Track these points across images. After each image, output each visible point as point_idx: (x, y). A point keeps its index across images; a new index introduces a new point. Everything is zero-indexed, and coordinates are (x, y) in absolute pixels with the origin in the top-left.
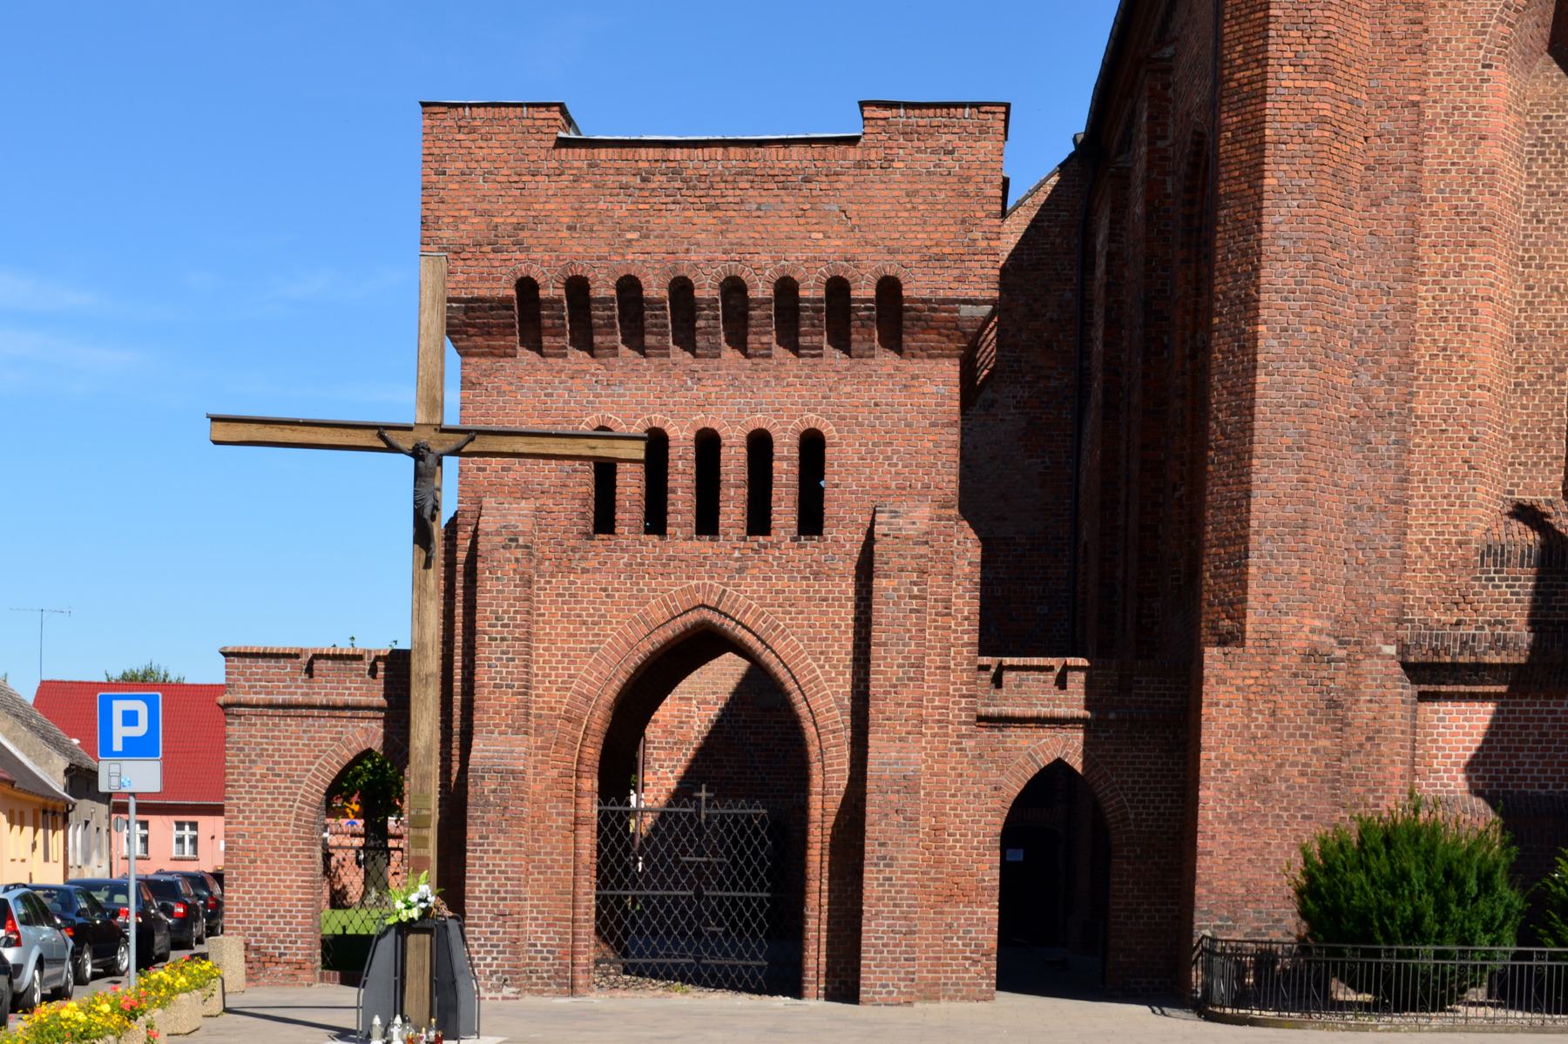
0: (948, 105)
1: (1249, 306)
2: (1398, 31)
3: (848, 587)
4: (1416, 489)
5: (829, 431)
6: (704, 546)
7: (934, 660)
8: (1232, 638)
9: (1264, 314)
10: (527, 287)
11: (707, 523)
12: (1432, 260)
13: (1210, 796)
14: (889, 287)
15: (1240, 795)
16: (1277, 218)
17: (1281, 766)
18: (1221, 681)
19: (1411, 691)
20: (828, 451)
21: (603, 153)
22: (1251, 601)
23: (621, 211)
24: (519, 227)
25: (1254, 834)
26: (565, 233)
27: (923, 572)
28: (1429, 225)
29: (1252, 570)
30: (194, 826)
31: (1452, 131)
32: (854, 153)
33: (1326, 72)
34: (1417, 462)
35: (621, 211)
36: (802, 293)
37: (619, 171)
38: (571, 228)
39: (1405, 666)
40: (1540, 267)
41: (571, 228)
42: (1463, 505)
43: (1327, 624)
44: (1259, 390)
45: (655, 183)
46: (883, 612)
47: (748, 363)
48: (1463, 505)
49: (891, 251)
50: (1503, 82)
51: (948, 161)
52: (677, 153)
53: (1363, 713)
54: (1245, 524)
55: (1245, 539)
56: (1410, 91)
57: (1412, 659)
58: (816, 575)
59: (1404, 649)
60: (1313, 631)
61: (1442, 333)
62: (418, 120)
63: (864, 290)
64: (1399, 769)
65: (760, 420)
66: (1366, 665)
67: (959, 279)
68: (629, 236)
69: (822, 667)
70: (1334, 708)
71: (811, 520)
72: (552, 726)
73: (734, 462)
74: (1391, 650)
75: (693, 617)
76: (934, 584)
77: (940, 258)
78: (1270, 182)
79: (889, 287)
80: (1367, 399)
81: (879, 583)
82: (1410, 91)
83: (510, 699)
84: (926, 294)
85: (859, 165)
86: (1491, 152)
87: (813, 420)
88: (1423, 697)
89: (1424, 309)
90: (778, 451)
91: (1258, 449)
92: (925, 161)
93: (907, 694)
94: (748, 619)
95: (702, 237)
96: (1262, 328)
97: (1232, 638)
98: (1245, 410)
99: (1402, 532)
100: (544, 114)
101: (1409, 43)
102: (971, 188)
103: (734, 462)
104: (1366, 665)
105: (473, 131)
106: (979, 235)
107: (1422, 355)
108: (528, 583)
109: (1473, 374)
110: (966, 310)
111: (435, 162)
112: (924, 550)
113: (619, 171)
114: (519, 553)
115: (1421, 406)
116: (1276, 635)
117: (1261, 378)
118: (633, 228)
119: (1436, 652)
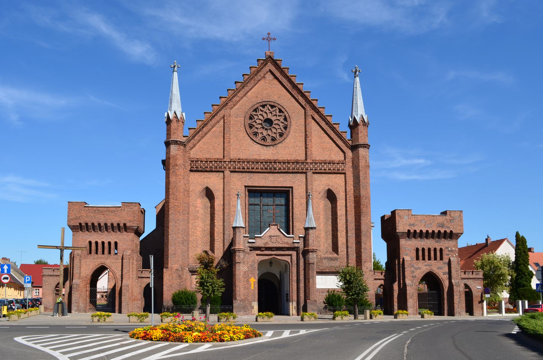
0: (132, 203)
1: (168, 227)
2: (186, 194)
3: (121, 261)
4: (190, 249)
5: (118, 242)
6: (103, 256)
7: (131, 270)
8: (167, 268)
9: (170, 228)
10: (80, 224)
11: (103, 253)
12: (191, 221)
13: (164, 287)
14: (125, 224)
15: (168, 287)
16: (171, 217)
17: (173, 283)
18: (166, 273)
19: (190, 274)
20: (118, 244)
21: (90, 208)
22: (169, 263)
23: (92, 215)
24: (79, 217)
25: (170, 292)
26: (85, 217)
27: (129, 259)
28: (191, 218)
29: (169, 259)
30: (39, 290)
31: (193, 206)
32: (120, 208)
33: (176, 200)
34: (190, 246)
35: (92, 215)
36: (114, 225)
37: (92, 210)
38: (86, 217)
39: (189, 271)
40: (206, 222)
41: (86, 217)
42: (196, 251)
43: (179, 266)
44: (169, 238)
45: (96, 211)
46: (124, 264)
47: (108, 233)
48: (196, 251)
49: (125, 220)
50: (199, 201)
51: (132, 209)
52: (99, 208)
53: (184, 277)
54: (168, 253)
55: (168, 255)
56: (187, 201)
57: (190, 270)
58: (117, 259)
59: (189, 269)
60: (177, 267)
61: (193, 230)
62: (67, 204)
63: (122, 225)
64: (189, 284)
65: (109, 240)
66: (184, 271)
67: (133, 224)
68: (93, 218)
70: (180, 277)
72: (83, 278)
73: (106, 245)
74: (187, 269)
75: (101, 265)
76: (131, 261)
77: (131, 221)
78: (170, 213)
79: (125, 224)
80: (184, 238)
81: (124, 261)
82: (187, 201)
83: (78, 275)
84: (129, 225)
85: (121, 210)
86: (198, 209)
87: (116, 240)
88: (192, 275)
89: (190, 227)
90: (112, 244)
91: (169, 245)
92: (129, 209)
93: (128, 274)
94: (108, 265)
95: (102, 218)
96: (169, 230)
97: (167, 268)
98: (168, 240)
99: (188, 254)
100: (83, 203)
101: (187, 196)
102: (135, 213)
103: (106, 245)
104: (184, 271)
105: (74, 205)
106: (135, 218)
107: (190, 233)
108: (80, 260)
109: (197, 235)
110: (134, 227)
111: (69, 209)
112: (129, 256)
113: (92, 210)
114: (79, 257)
115: (190, 239)
116: (172, 267)
117: (170, 236)
118: (93, 217)
119: (193, 269)
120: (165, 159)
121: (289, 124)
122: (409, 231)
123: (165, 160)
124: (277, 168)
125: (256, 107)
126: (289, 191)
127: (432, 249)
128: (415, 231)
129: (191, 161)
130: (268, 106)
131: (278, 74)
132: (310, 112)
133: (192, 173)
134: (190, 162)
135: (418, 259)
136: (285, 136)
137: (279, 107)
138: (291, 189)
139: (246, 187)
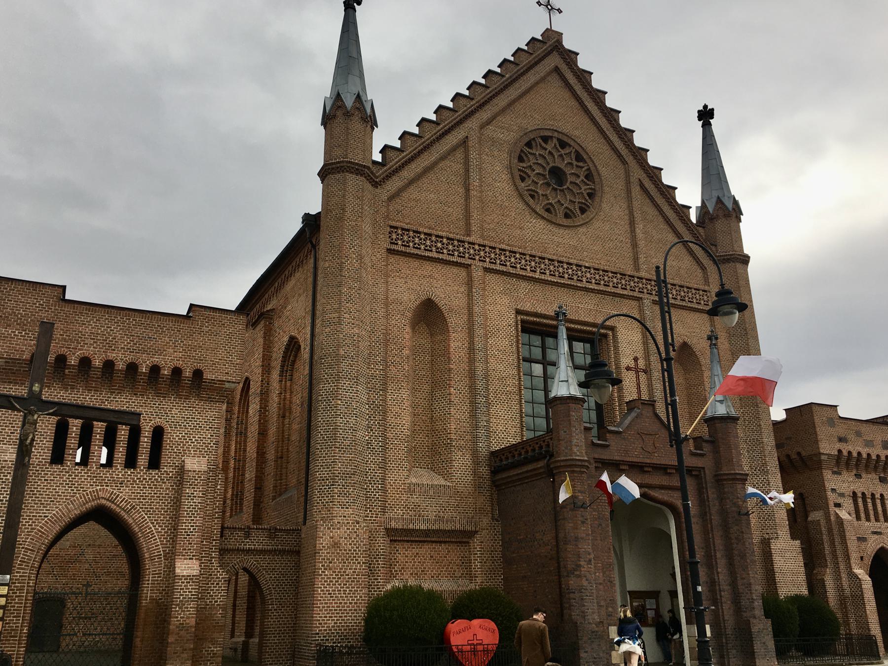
69: (154, 526)
71: (154, 463)
87: (158, 421)
120: (319, 210)
121: (598, 187)
122: (840, 451)
123: (319, 213)
124: (584, 279)
125: (532, 137)
126: (605, 336)
127: (878, 496)
128: (850, 453)
129: (391, 227)
130: (555, 140)
131: (572, 80)
132: (637, 173)
133: (393, 259)
134: (389, 229)
135: (858, 518)
136: (589, 214)
137: (577, 148)
138: (610, 333)
139: (518, 312)
